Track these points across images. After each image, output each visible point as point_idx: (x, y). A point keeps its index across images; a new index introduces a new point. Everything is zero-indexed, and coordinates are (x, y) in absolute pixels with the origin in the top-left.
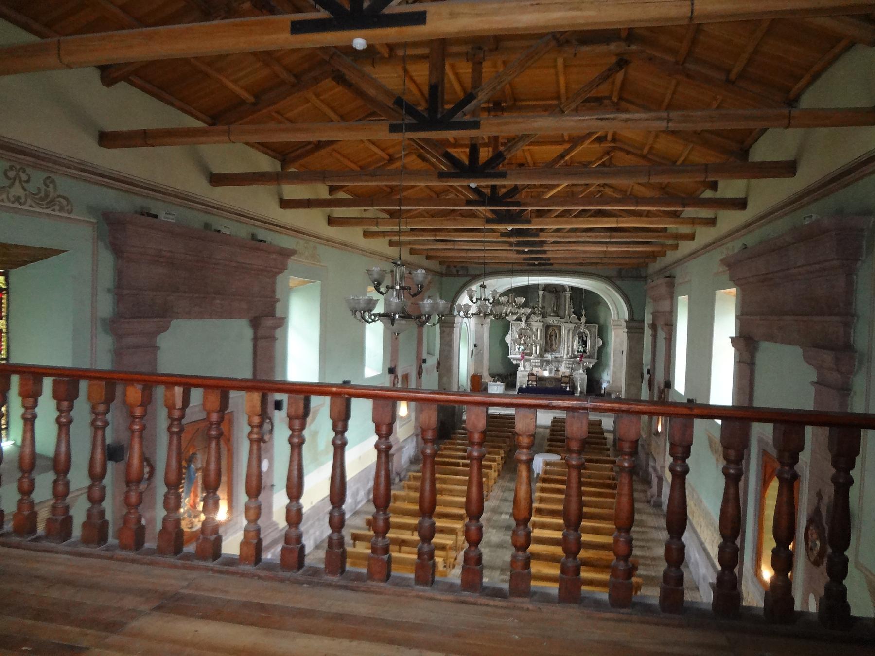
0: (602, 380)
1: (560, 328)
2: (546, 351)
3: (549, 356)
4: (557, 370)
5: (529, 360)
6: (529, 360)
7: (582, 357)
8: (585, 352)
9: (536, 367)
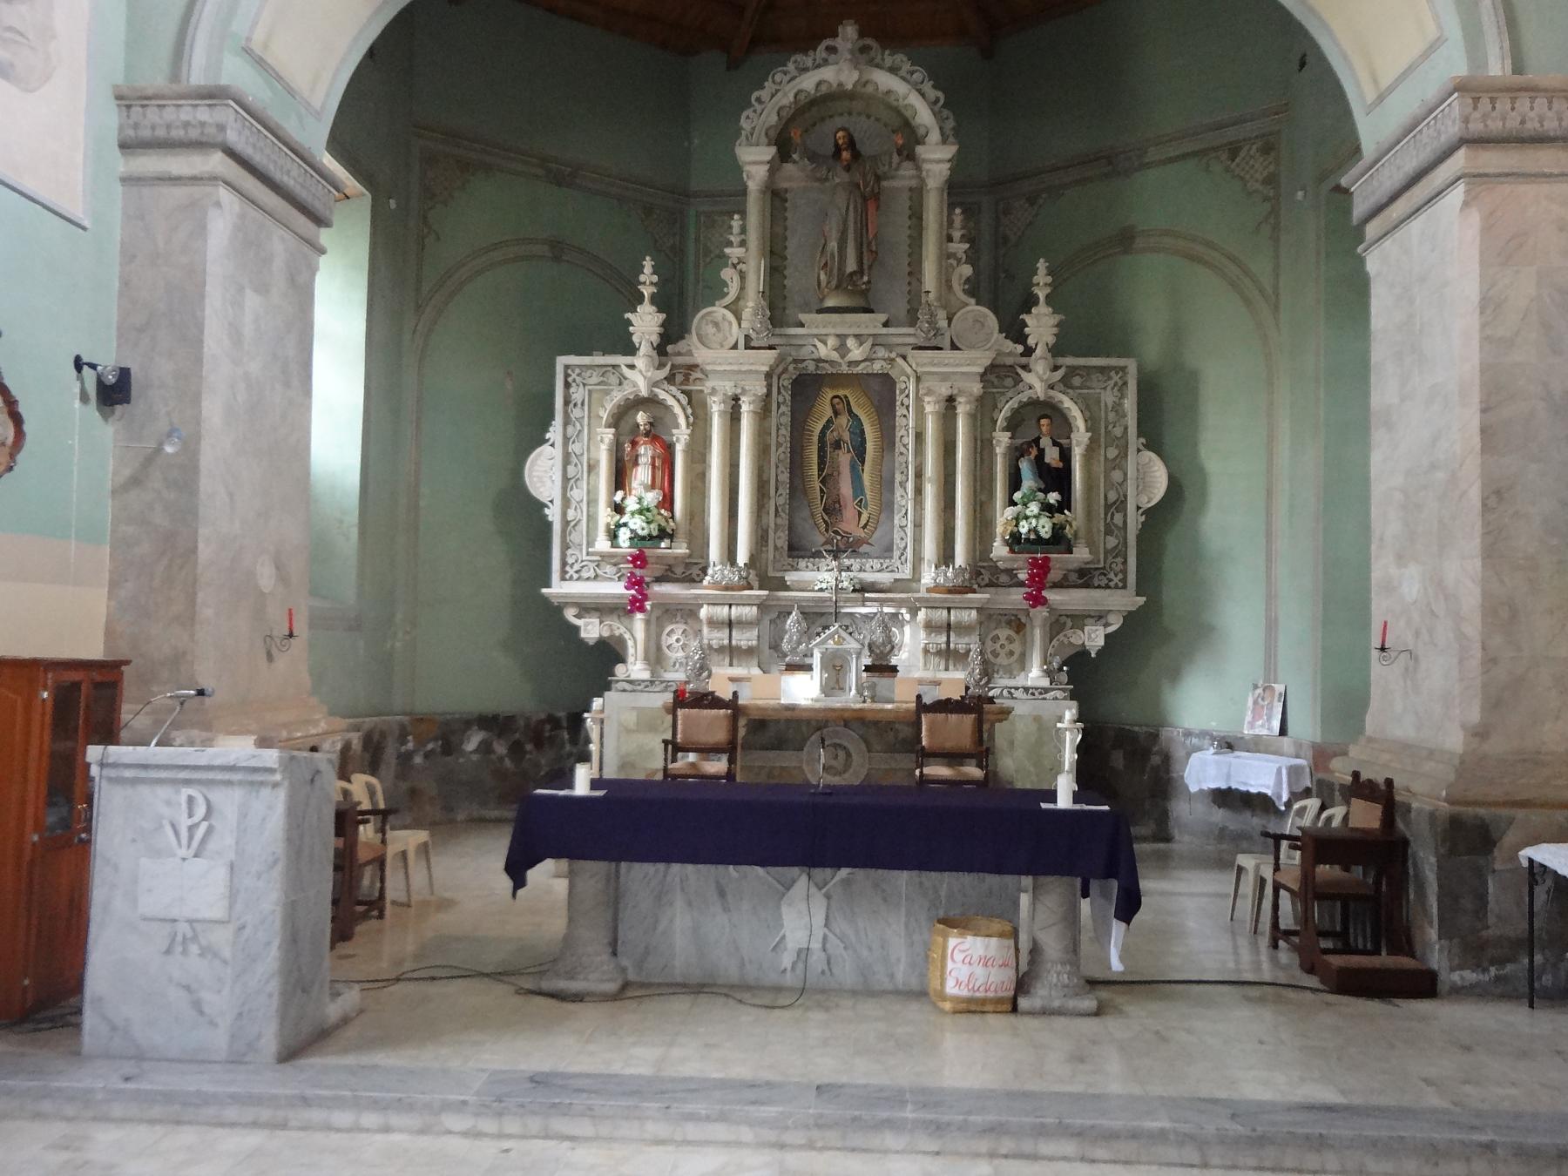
0: (1172, 735)
1: (883, 393)
2: (797, 550)
3: (819, 578)
4: (882, 668)
5: (687, 612)
6: (687, 612)
7: (1040, 573)
8: (1059, 540)
9: (733, 653)
